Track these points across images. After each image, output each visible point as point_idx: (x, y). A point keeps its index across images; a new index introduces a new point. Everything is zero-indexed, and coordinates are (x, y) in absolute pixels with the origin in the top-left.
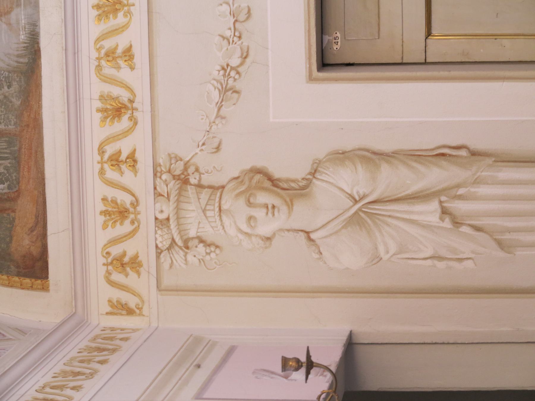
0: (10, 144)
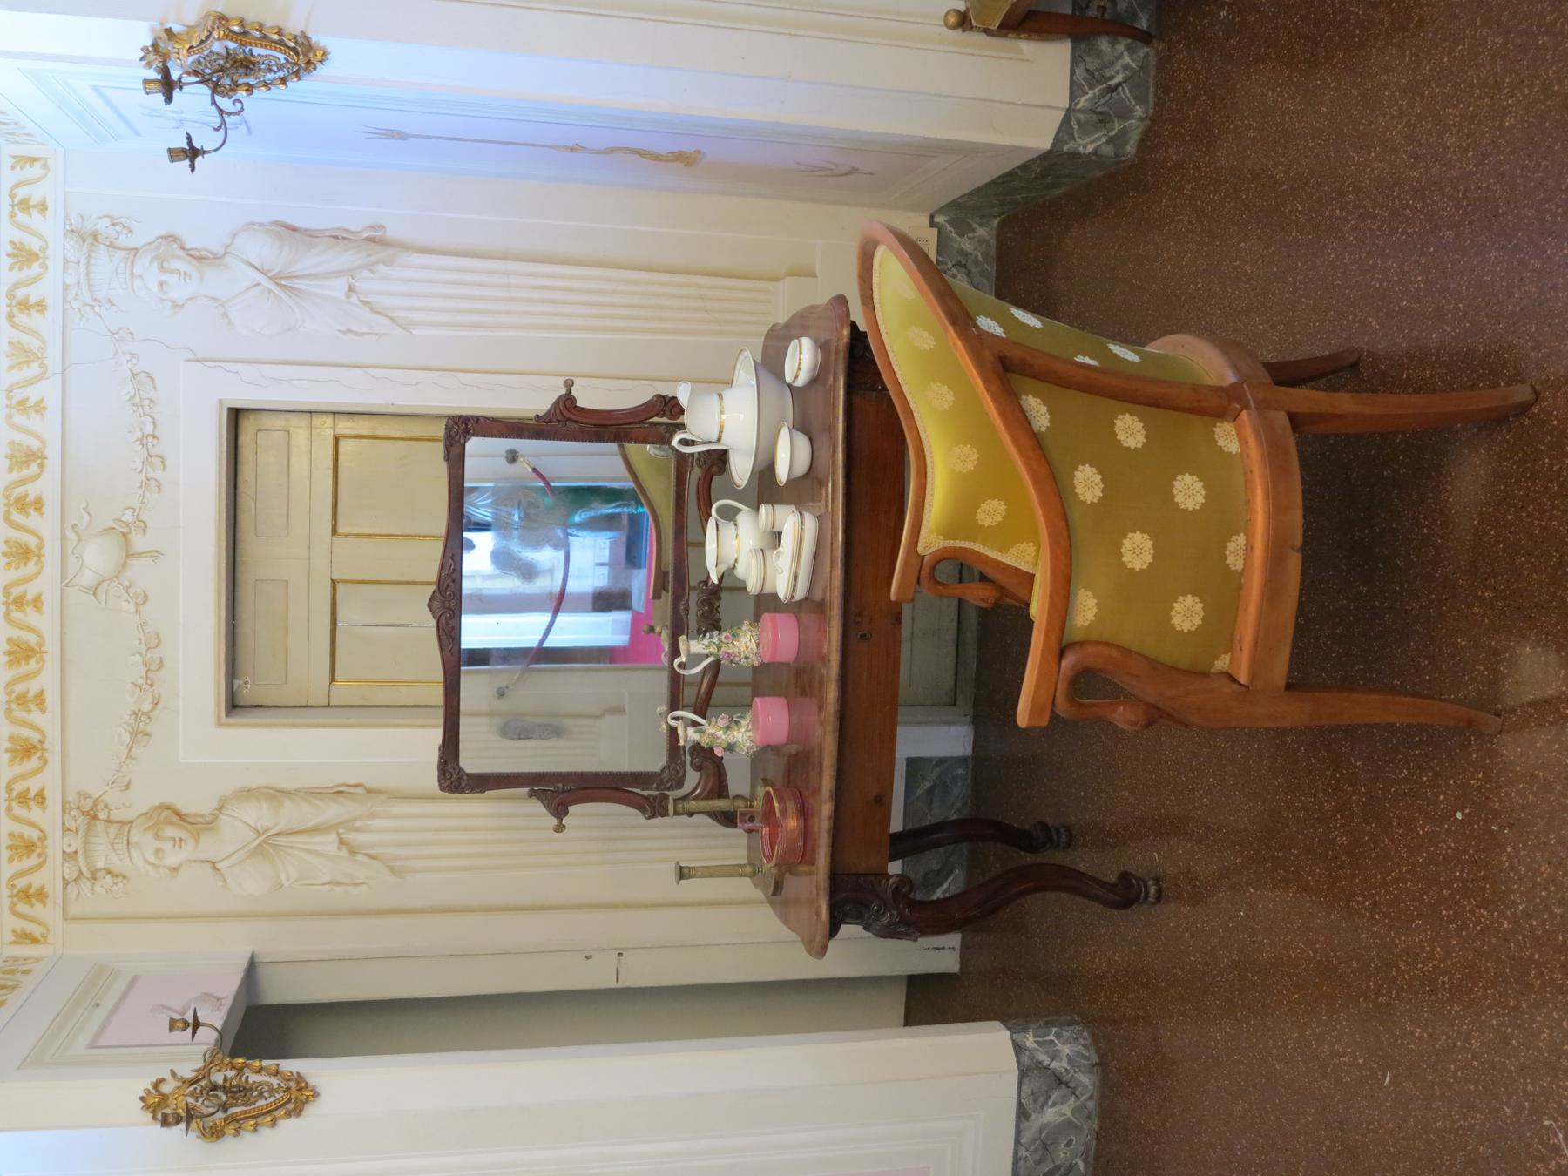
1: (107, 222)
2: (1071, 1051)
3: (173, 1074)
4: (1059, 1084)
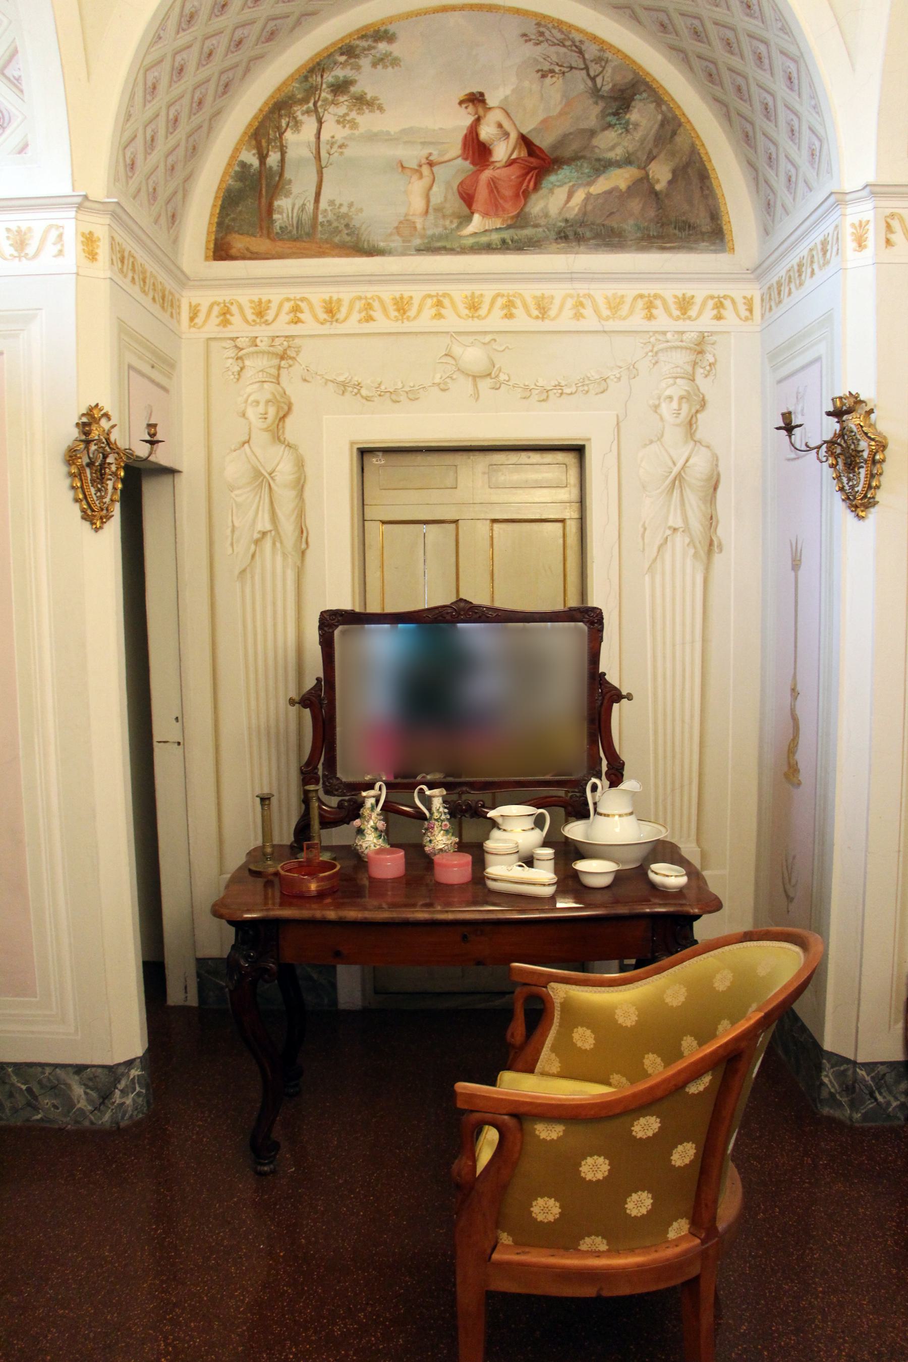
0: (308, 234)
1: (712, 360)
3: (113, 426)
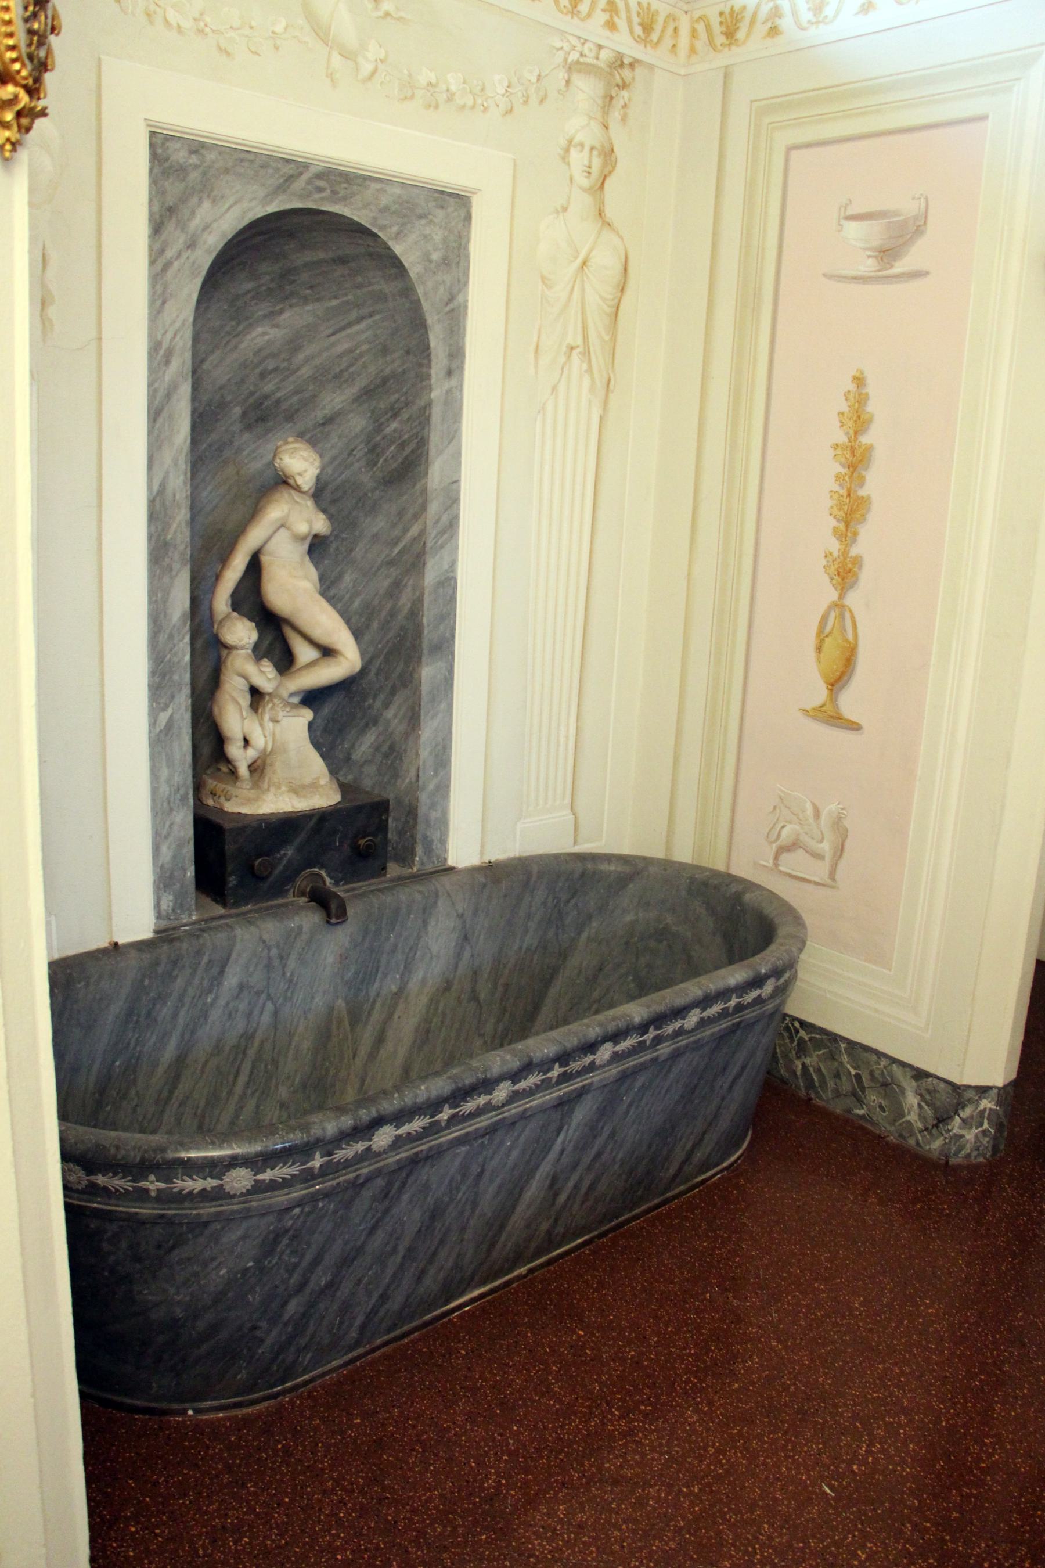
2: (967, 1141)
4: (938, 1119)
